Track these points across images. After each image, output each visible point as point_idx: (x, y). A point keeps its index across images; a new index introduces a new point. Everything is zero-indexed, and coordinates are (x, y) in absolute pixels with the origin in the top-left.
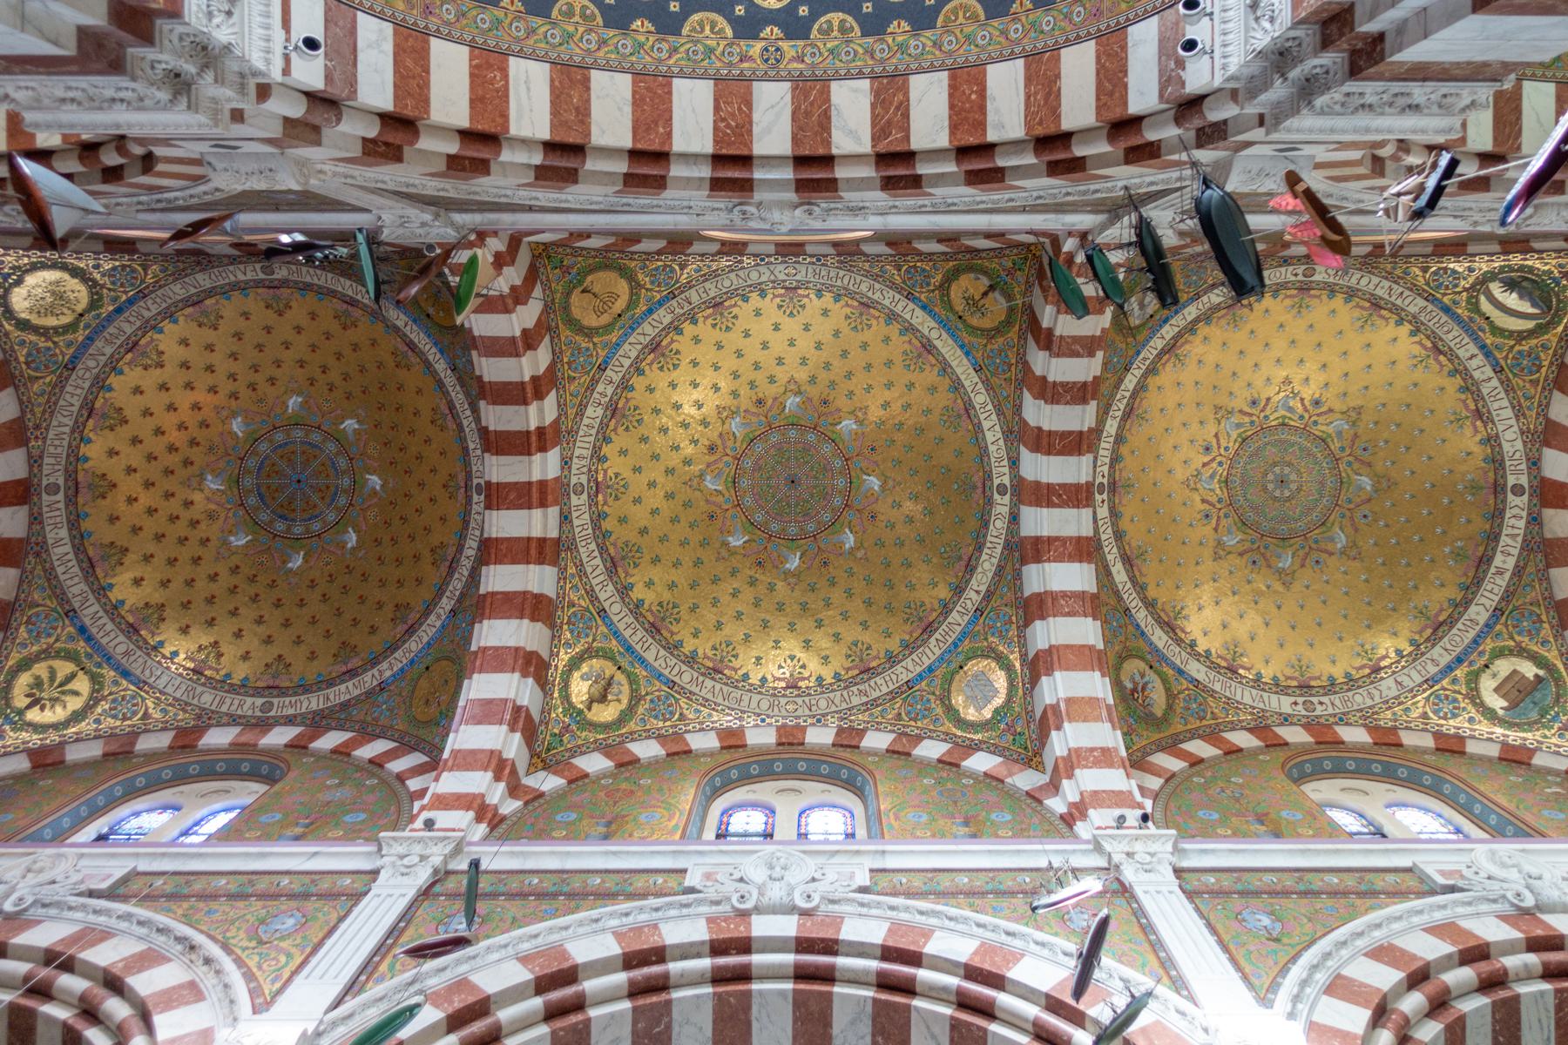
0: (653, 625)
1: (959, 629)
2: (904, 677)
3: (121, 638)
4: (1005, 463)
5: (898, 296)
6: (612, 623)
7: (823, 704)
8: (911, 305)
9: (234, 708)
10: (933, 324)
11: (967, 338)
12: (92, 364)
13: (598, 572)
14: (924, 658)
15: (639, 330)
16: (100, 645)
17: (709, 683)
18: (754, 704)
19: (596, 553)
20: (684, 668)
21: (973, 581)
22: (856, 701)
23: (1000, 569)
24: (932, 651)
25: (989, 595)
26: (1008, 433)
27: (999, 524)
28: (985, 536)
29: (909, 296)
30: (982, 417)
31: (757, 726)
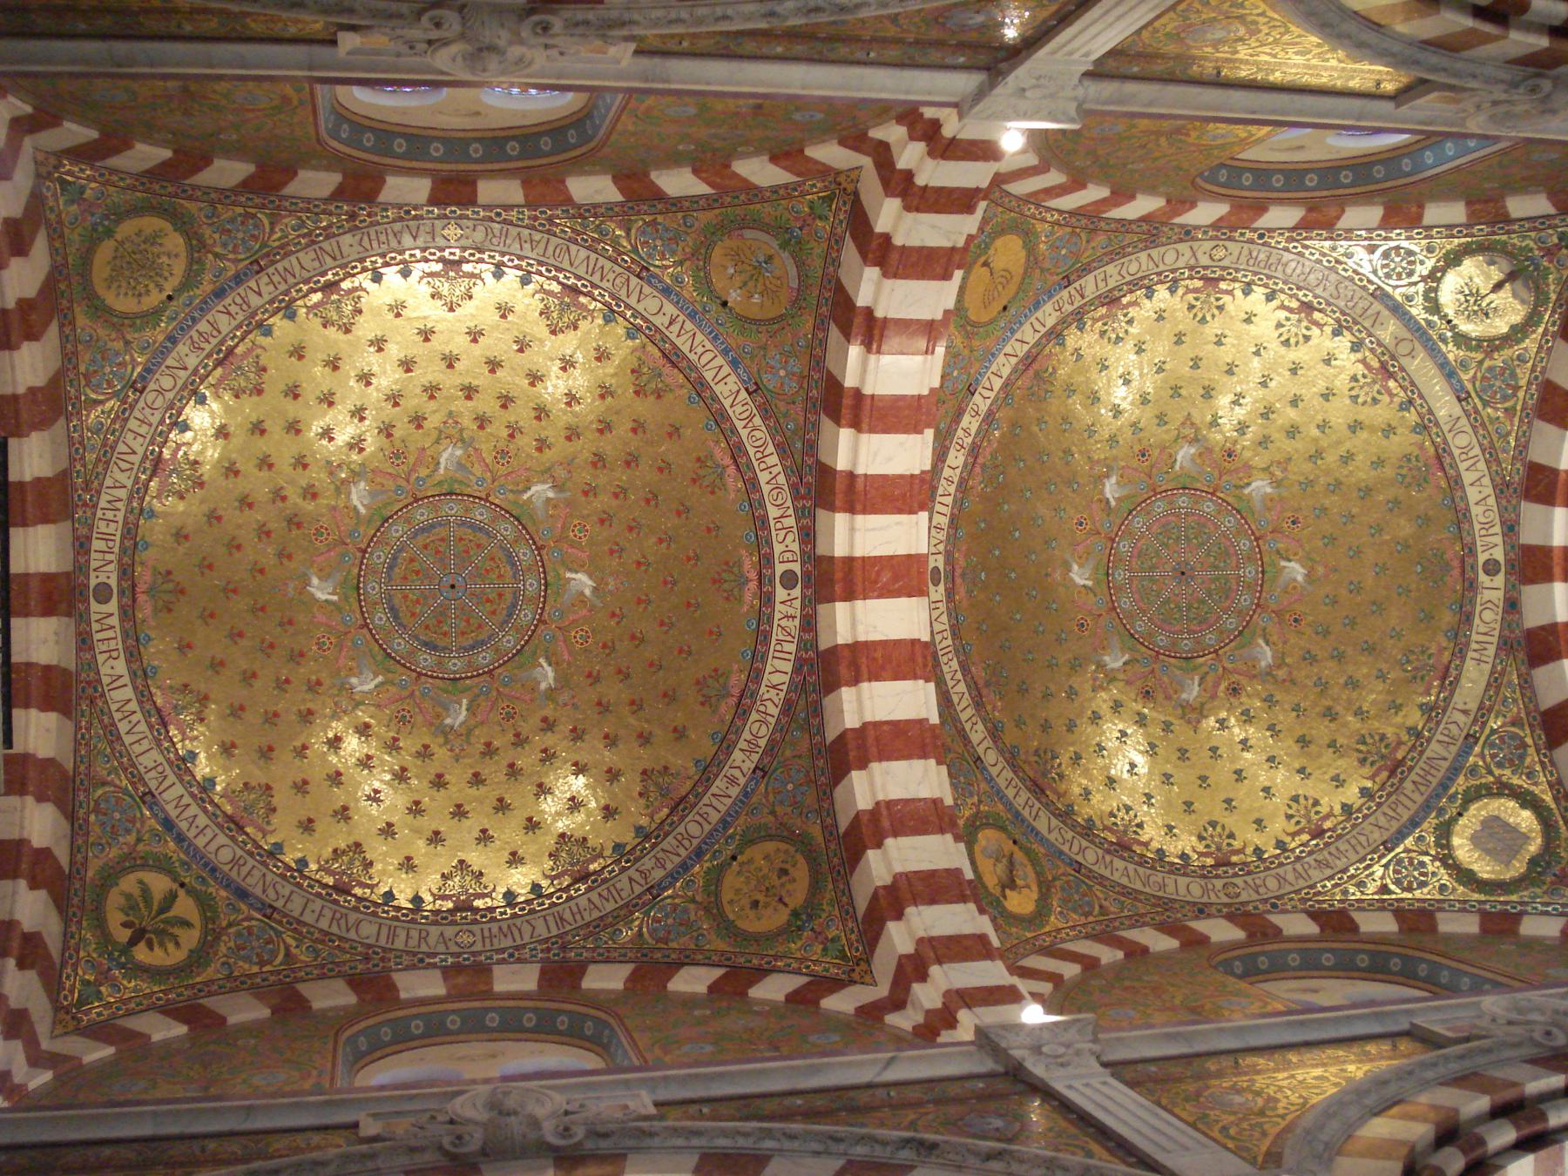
1: (1445, 764)
2: (1377, 836)
3: (222, 839)
4: (1498, 529)
7: (1272, 883)
8: (1377, 306)
9: (413, 943)
11: (1452, 352)
12: (167, 383)
13: (964, 703)
15: (1018, 336)
16: (196, 848)
17: (1119, 864)
18: (1182, 891)
20: (1085, 843)
23: (1495, 682)
25: (1483, 712)
26: (1502, 488)
27: (1488, 616)
30: (1462, 466)
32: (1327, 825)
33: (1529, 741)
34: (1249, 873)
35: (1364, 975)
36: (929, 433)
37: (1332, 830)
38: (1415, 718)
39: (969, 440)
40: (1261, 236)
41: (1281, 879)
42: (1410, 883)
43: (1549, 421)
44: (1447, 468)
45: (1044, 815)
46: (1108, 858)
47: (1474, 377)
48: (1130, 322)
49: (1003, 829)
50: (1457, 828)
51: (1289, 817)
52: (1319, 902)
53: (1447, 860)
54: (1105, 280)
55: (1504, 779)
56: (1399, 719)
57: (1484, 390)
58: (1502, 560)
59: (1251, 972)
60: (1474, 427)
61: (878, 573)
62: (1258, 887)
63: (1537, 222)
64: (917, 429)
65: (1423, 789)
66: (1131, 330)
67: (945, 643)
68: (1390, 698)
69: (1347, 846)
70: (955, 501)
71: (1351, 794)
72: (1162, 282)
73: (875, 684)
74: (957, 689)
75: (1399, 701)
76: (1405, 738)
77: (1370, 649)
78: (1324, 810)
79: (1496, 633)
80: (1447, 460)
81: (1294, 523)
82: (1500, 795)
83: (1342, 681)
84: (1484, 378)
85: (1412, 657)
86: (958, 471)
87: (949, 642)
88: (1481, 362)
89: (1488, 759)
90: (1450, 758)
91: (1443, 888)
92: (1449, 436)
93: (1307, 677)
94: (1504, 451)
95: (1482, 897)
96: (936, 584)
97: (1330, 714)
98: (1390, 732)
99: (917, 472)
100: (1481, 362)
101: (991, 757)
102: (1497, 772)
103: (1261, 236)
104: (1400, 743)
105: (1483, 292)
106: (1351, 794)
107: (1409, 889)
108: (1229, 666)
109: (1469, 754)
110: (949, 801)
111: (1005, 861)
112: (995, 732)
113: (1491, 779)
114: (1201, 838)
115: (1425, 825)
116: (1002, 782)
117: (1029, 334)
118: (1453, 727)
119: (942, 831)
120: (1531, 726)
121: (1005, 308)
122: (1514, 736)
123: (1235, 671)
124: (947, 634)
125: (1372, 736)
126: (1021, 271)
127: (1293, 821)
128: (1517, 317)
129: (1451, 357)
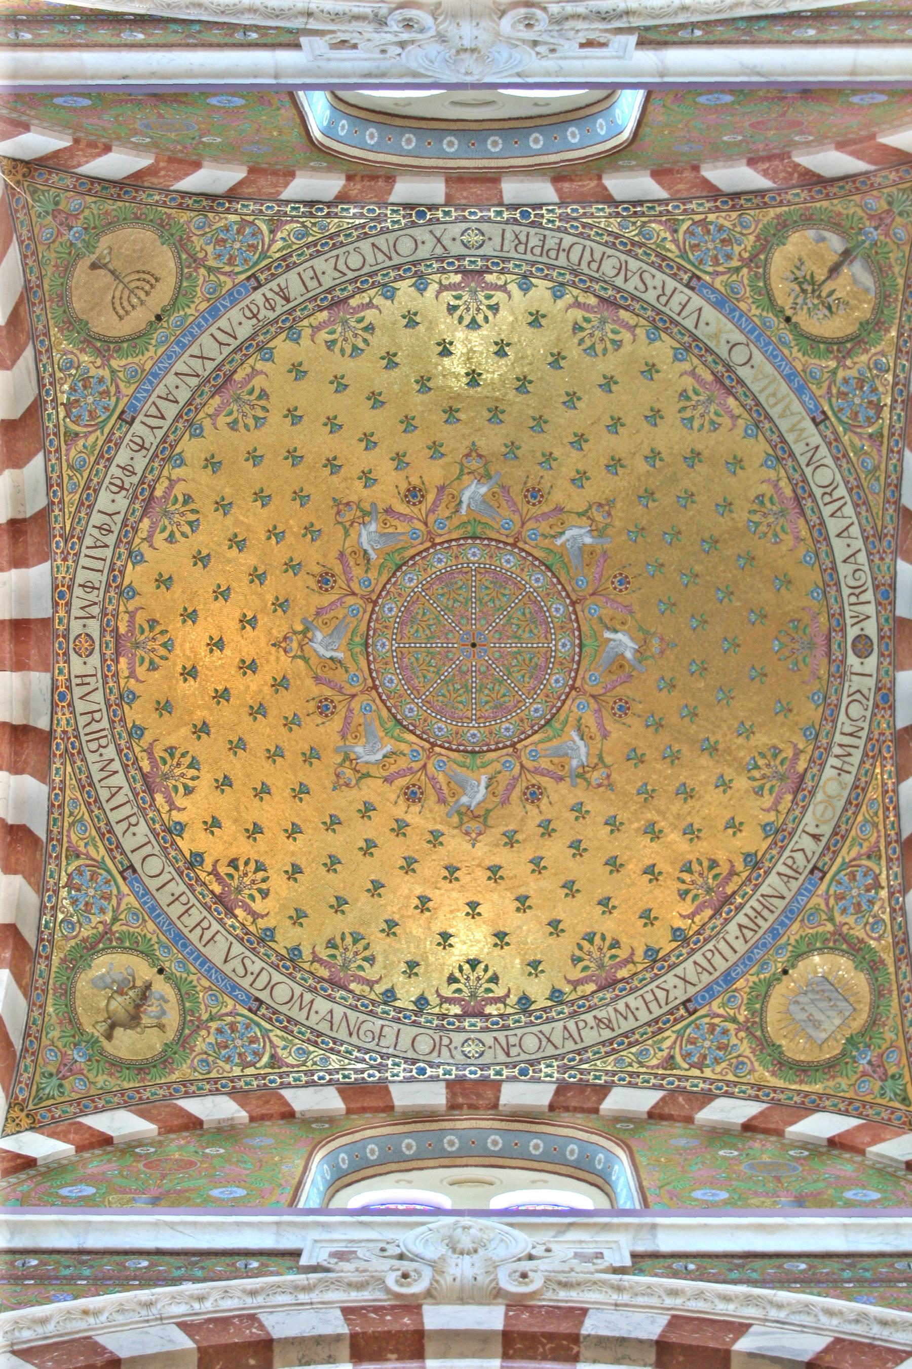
1: (780, 904)
2: (680, 994)
4: (869, 596)
5: (671, 284)
6: (147, 891)
7: (531, 1043)
8: (697, 301)
10: (737, 337)
11: (799, 359)
13: (120, 799)
14: (717, 960)
15: (194, 350)
17: (322, 1005)
19: (116, 765)
20: (277, 977)
21: (809, 818)
22: (591, 1037)
28: (831, 734)
29: (693, 283)
30: (827, 511)
31: (410, 1080)
34: (506, 1028)
35: (571, 1171)
39: (135, 479)
40: (525, 215)
46: (308, 997)
47: (829, 391)
54: (315, 277)
65: (749, 934)
69: (640, 1003)
79: (864, 734)
80: (809, 503)
86: (119, 519)
90: (789, 896)
92: (808, 471)
93: (629, 781)
98: (721, 856)
100: (834, 372)
105: (820, 277)
107: (700, 1066)
108: (529, 764)
115: (741, 983)
121: (159, 318)
123: (537, 771)
125: (700, 864)
127: (580, 965)
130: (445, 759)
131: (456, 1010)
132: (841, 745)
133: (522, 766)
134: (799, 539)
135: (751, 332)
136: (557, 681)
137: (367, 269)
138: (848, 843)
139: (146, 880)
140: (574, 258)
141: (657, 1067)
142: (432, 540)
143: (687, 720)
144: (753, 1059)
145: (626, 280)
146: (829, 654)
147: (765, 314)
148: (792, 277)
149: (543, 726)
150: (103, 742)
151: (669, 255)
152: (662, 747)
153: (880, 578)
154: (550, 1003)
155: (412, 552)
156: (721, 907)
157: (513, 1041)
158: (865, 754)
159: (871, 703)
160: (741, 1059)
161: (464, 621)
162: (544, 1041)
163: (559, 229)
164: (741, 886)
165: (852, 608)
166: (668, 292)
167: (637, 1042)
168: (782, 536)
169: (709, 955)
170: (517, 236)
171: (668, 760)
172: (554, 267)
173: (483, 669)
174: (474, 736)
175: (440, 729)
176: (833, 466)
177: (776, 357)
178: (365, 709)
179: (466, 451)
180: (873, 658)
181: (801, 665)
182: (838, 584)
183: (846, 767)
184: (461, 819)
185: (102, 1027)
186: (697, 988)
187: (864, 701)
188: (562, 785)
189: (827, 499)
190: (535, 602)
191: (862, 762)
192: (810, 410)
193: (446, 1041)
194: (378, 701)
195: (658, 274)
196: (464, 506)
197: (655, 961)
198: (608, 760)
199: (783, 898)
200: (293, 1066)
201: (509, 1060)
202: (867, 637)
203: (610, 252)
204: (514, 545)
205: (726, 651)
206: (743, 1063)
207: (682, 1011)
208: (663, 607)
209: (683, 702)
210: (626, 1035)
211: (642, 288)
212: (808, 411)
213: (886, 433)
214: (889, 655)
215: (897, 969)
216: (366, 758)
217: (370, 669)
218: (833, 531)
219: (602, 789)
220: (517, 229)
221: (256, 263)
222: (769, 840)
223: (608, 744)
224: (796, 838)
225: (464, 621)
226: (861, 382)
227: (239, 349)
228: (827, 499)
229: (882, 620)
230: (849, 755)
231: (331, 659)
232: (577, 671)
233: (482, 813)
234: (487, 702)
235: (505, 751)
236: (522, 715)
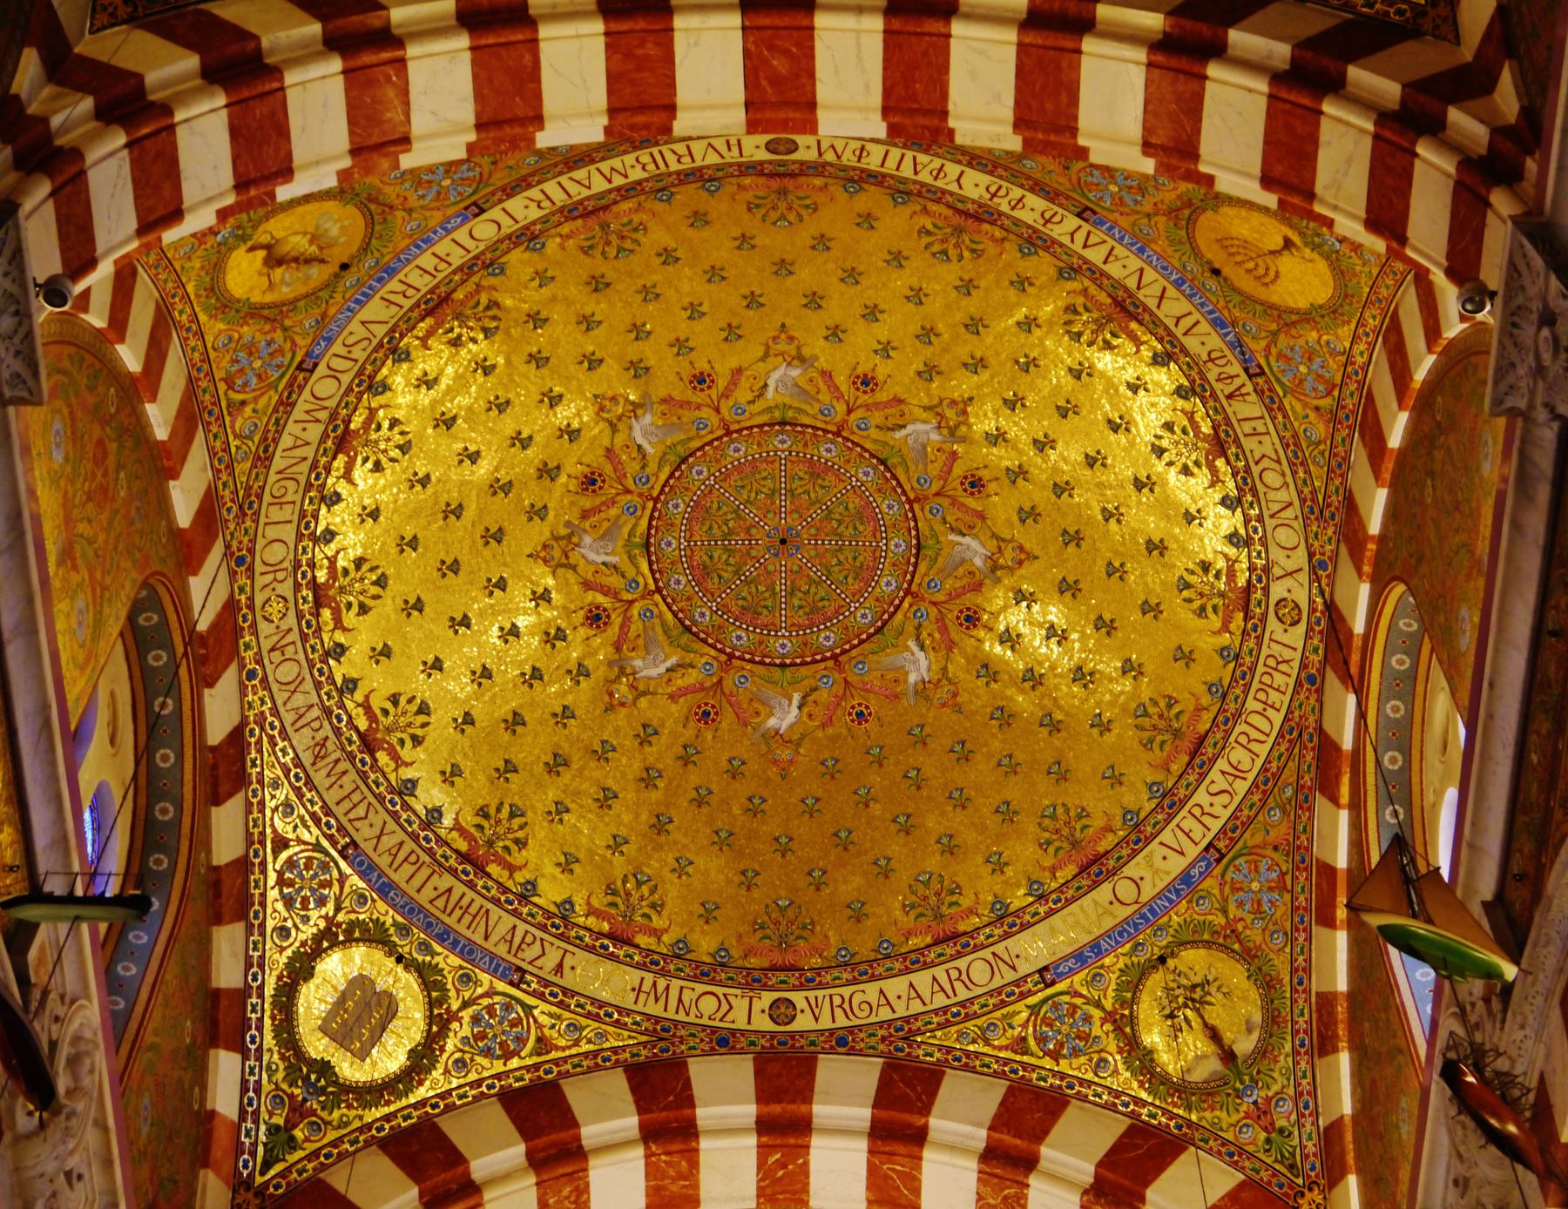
0: (445, 299)
1: (478, 938)
2: (364, 834)
4: (842, 1021)
5: (1216, 826)
7: (288, 672)
8: (1193, 852)
10: (1148, 892)
11: (1114, 962)
13: (573, 188)
14: (408, 869)
15: (1172, 292)
17: (314, 432)
18: (271, 533)
20: (346, 379)
24: (428, 887)
25: (563, 997)
26: (905, 1029)
27: (709, 1005)
29: (1213, 853)
30: (939, 972)
32: (383, 758)
33: (514, 1063)
34: (304, 638)
35: (141, 813)
36: (1014, 143)
37: (375, 766)
38: (551, 893)
39: (1005, 208)
40: (1311, 679)
41: (294, 686)
42: (291, 884)
43: (1002, 1103)
44: (939, 949)
45: (390, 314)
46: (323, 415)
47: (1078, 994)
48: (1186, 471)
49: (365, 248)
50: (378, 954)
51: (394, 699)
52: (259, 742)
53: (328, 939)
54: (1255, 433)
55: (455, 1025)
56: (550, 869)
57: (1056, 1006)
58: (795, 1026)
59: (138, 640)
60: (999, 991)
61: (786, 52)
62: (282, 650)
63: (1307, 1099)
64: (1021, 123)
65: (440, 903)
66: (1173, 471)
67: (671, 159)
68: (581, 856)
69: (348, 787)
70: (904, 181)
71: (430, 794)
72: (1247, 521)
73: (601, 41)
74: (596, 177)
75: (576, 867)
76: (520, 877)
77: (660, 825)
78: (406, 753)
79: (682, 1017)
80: (949, 950)
81: (860, 715)
82: (431, 1019)
83: (610, 783)
84: (1075, 1007)
85: (645, 890)
86: (954, 188)
87: (674, 166)
88: (1098, 1005)
89: (485, 1002)
91: (283, 932)
92: (986, 953)
93: (617, 730)
94: (961, 1034)
95: (269, 991)
96: (769, 147)
97: (557, 764)
99: (952, 123)
101: (485, 230)
102: (466, 1015)
103: (1311, 679)
104: (512, 869)
106: (430, 794)
107: (281, 882)
109: (494, 973)
110: (407, 161)
111: (313, 249)
112: (527, 237)
113: (455, 1006)
114: (359, 562)
115: (382, 906)
116: (443, 247)
117: (1174, 307)
118: (537, 949)
119: (355, 152)
120: (536, 1067)
121: (1216, 272)
122: (521, 1041)
124: (687, 163)
125: (521, 828)
126: (1275, 299)
127: (388, 706)
128: (1167, 1061)
129: (1107, 961)
130: (639, 513)
131: (322, 576)
132: (667, 988)
133: (631, 602)
134: (908, 935)
135: (1151, 910)
136: (739, 638)
137: (1260, 488)
138: (554, 1009)
139: (467, 227)
140: (1256, 720)
141: (275, 831)
142: (917, 500)
143: (694, 794)
144: (294, 948)
145: (1223, 773)
146: (774, 968)
147: (1171, 931)
148: (1210, 978)
149: (683, 624)
150: (651, 167)
151: (1247, 835)
152: (660, 766)
153: (862, 1035)
154: (339, 682)
155: (902, 478)
156: (471, 862)
157: (289, 651)
158: (658, 1020)
159: (716, 1024)
160: (293, 932)
161: (813, 531)
162: (292, 687)
163: (1289, 711)
164: (497, 882)
165: (827, 999)
166: (1205, 819)
167: (300, 796)
168: (913, 914)
169: (413, 858)
170: (1287, 662)
171: (644, 775)
172: (1246, 692)
173: (754, 553)
174: (669, 544)
175: (676, 506)
176: (993, 986)
177: (1121, 934)
178: (701, 425)
179: (1028, 546)
180: (769, 1026)
181: (759, 934)
182: (854, 981)
183: (642, 997)
184: (562, 538)
185: (264, 239)
186: (370, 852)
187: (719, 1015)
188: (611, 650)
189: (954, 974)
190: (837, 612)
191: (648, 1017)
192: (1057, 967)
193: (280, 576)
194: (710, 437)
195: (1227, 813)
196: (958, 538)
197: (400, 794)
198: (643, 702)
199: (486, 938)
200: (233, 427)
201: (265, 653)
202: (794, 1017)
203: (1259, 763)
204: (908, 592)
205: (776, 839)
206: (288, 935)
207: (343, 841)
208: (830, 763)
209: (714, 788)
210: (309, 783)
211: (1214, 789)
212: (1056, 964)
213: (1025, 1059)
214: (772, 1046)
215: (415, 1106)
216: (636, 427)
217: (751, 428)
218: (915, 978)
219: (607, 698)
220: (1296, 665)
221: (1278, 380)
222: (553, 909)
223: (664, 701)
224: (557, 942)
225: (813, 531)
226: (1085, 1037)
227: (1170, 333)
228: (954, 974)
229: (812, 1037)
230: (657, 1000)
231: (766, 385)
232: (751, 661)
233: (572, 561)
234: (711, 557)
235: (651, 581)
236: (696, 598)
